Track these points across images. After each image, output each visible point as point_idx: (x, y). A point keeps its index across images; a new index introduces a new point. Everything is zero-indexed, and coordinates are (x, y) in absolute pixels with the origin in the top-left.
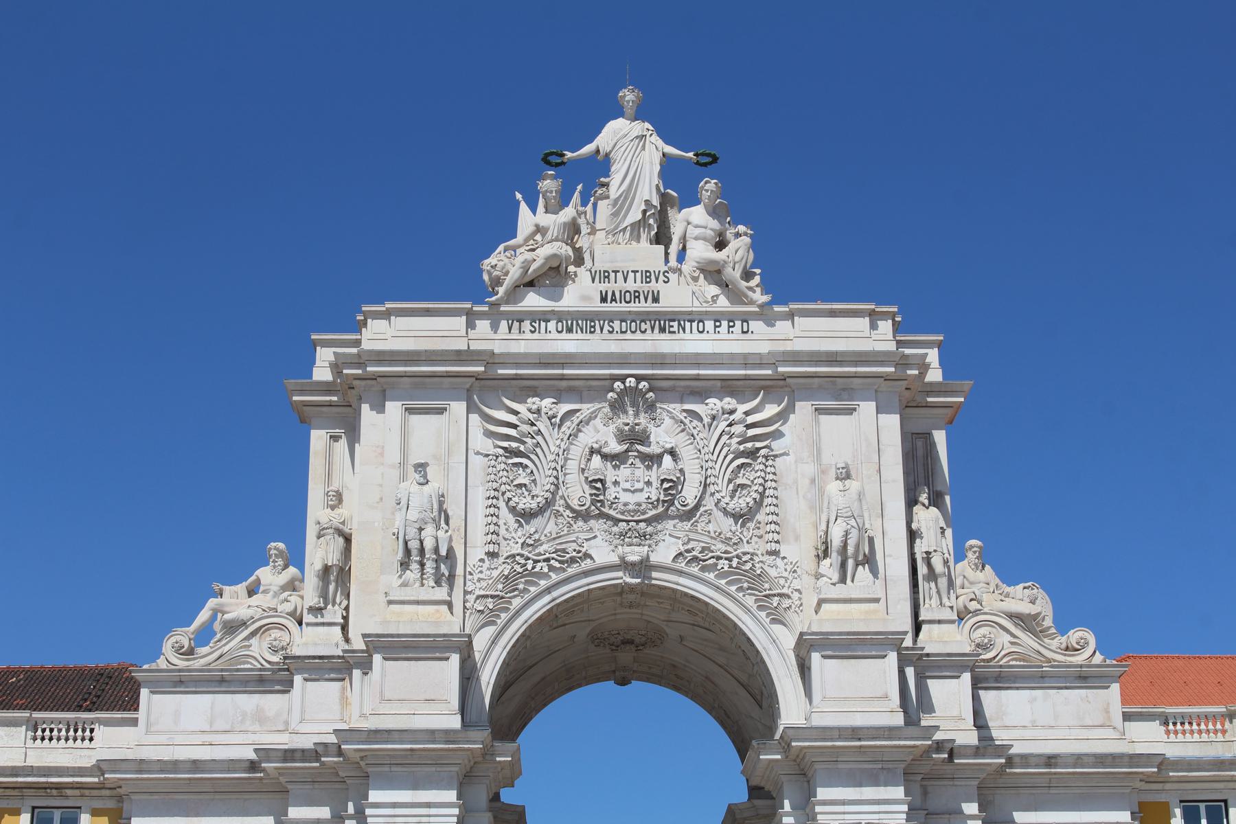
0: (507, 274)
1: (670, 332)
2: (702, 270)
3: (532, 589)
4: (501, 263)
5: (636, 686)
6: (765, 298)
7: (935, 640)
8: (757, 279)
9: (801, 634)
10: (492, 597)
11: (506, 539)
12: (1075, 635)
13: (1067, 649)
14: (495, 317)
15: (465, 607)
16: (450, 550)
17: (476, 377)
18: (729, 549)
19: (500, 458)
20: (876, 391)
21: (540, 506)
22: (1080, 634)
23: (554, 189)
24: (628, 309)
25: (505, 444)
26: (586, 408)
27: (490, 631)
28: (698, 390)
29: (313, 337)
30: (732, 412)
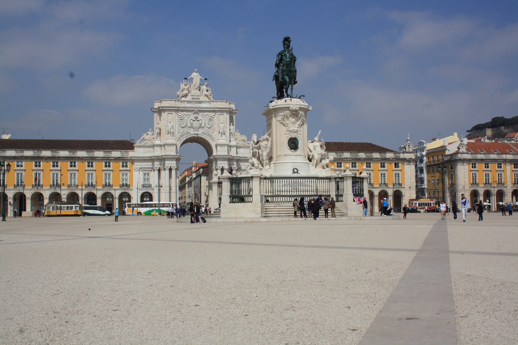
3: (184, 137)
5: (194, 143)
7: (233, 143)
8: (212, 96)
26: (190, 113)
28: (204, 111)
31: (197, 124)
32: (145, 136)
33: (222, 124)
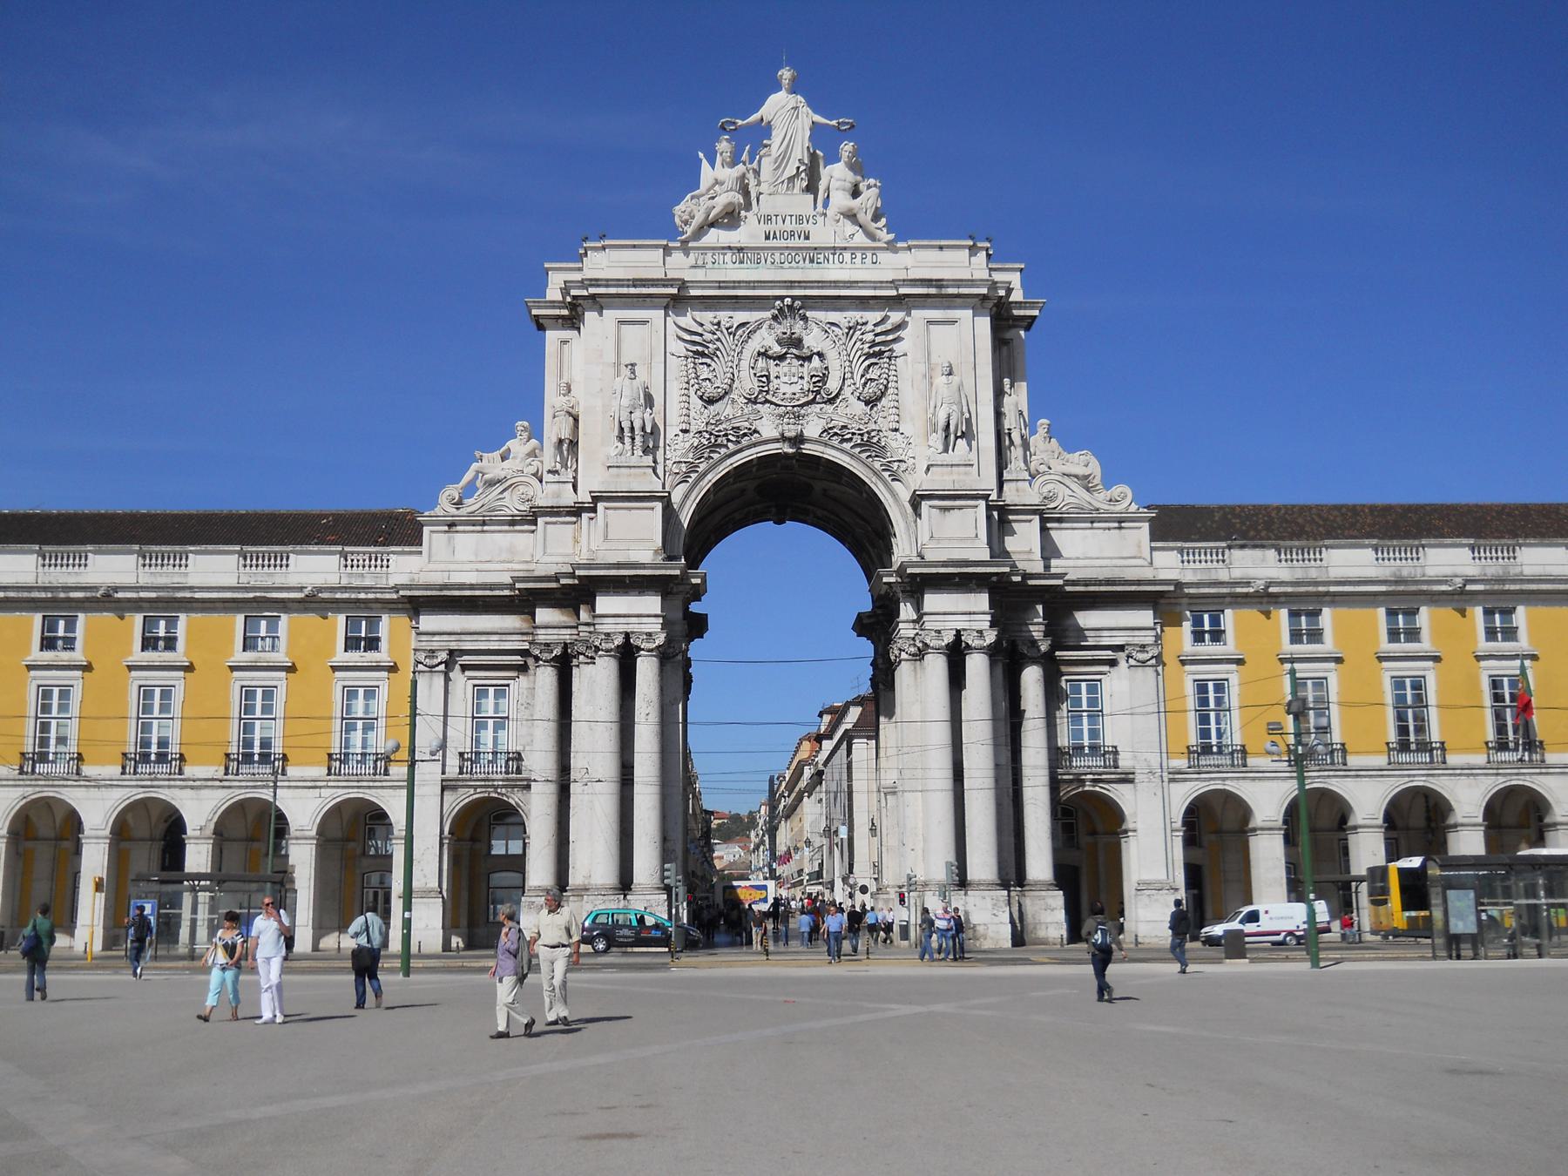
0: (693, 218)
1: (817, 263)
2: (841, 214)
3: (715, 456)
4: (689, 209)
6: (891, 236)
9: (915, 491)
10: (685, 462)
12: (1117, 490)
13: (1110, 501)
14: (685, 249)
15: (665, 471)
16: (655, 426)
17: (673, 297)
18: (861, 427)
19: (689, 360)
20: (973, 308)
22: (1120, 490)
23: (729, 150)
24: (785, 245)
25: (694, 348)
27: (683, 488)
29: (546, 266)
30: (865, 324)
31: (795, 379)
32: (491, 465)
33: (950, 374)
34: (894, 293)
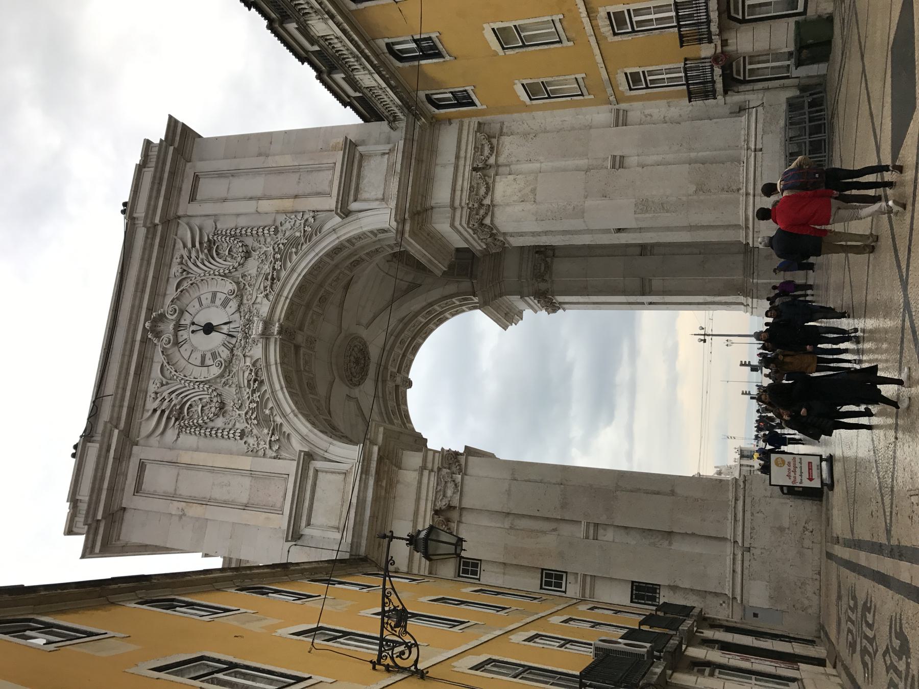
3: (270, 405)
5: (412, 376)
11: (235, 425)
19: (182, 424)
20: (190, 162)
21: (216, 394)
25: (173, 419)
30: (182, 257)
34: (160, 228)
